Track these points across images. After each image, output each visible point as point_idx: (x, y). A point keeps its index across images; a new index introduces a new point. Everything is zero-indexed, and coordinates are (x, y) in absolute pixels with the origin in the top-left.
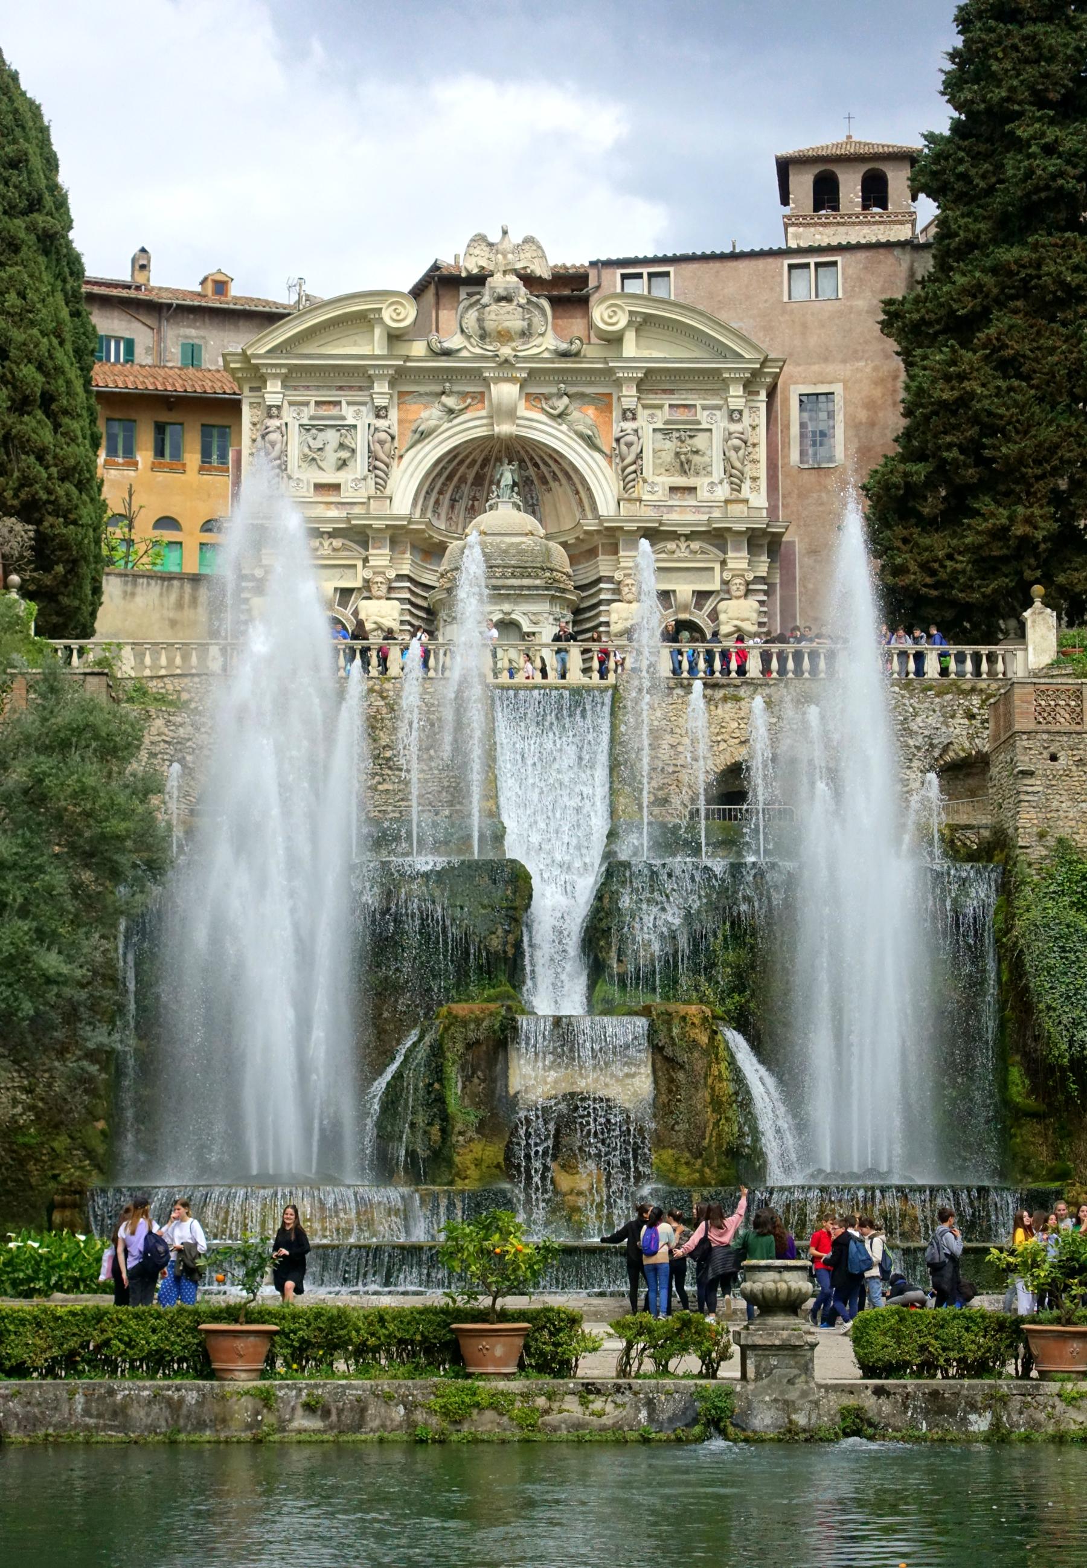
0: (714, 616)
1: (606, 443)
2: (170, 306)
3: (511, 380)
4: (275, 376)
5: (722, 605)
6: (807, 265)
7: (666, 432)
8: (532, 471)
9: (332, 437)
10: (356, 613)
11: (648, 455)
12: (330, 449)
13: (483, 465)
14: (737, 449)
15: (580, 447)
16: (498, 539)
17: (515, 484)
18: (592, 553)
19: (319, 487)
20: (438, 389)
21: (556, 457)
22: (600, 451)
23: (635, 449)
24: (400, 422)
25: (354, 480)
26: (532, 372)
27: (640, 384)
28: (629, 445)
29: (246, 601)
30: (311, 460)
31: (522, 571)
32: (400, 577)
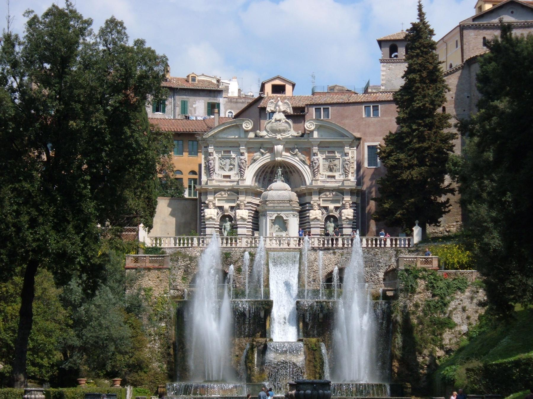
0: (340, 213)
2: (177, 89)
5: (343, 211)
8: (287, 169)
9: (228, 161)
10: (235, 213)
12: (227, 165)
13: (273, 168)
15: (301, 164)
16: (277, 192)
17: (282, 174)
18: (304, 195)
22: (307, 165)
23: (317, 164)
24: (248, 156)
28: (315, 163)
29: (203, 210)
31: (283, 201)
32: (248, 203)
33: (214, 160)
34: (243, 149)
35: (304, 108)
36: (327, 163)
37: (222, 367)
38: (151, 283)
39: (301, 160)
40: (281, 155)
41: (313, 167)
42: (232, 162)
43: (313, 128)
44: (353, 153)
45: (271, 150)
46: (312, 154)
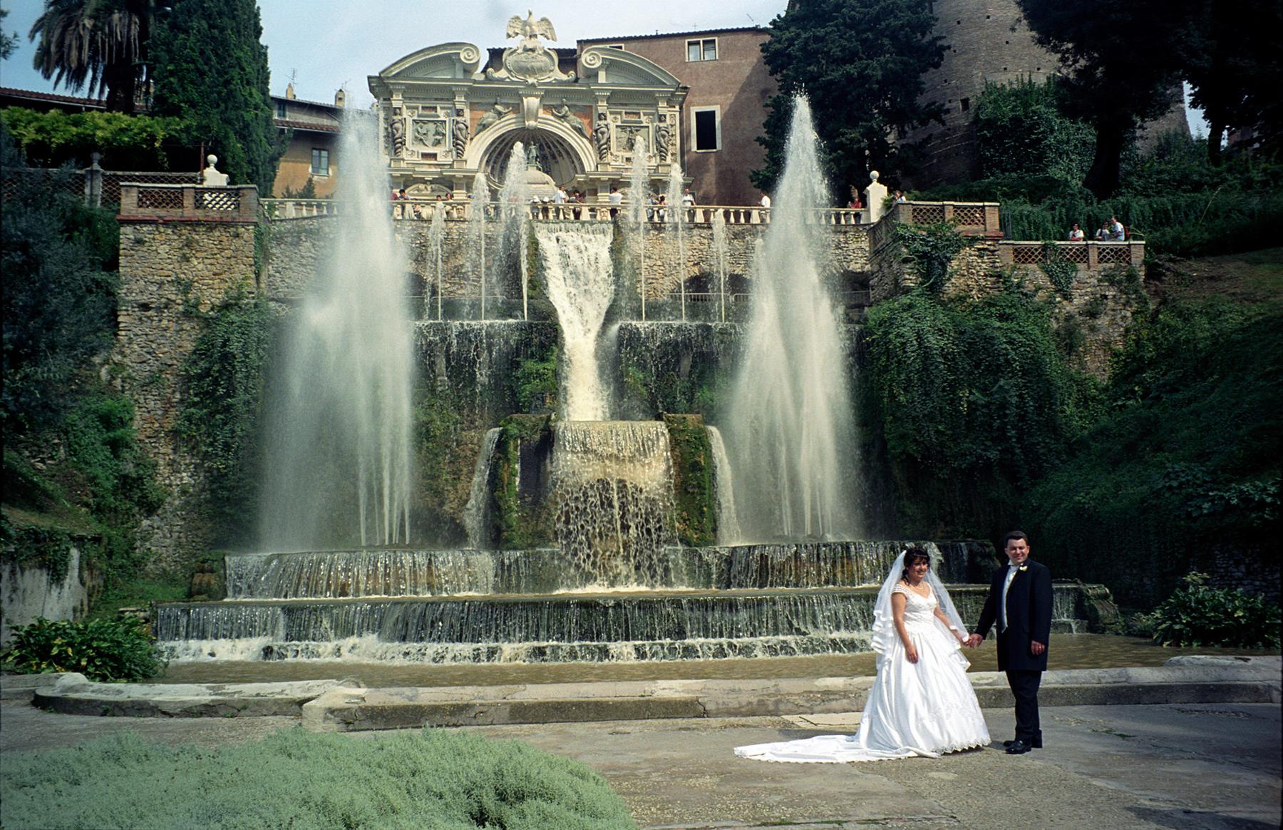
1: (588, 132)
3: (536, 96)
4: (398, 90)
6: (698, 43)
7: (623, 128)
8: (547, 151)
9: (431, 127)
11: (613, 139)
14: (664, 136)
15: (575, 135)
19: (425, 156)
20: (493, 101)
21: (561, 141)
24: (472, 119)
25: (444, 153)
26: (547, 91)
27: (608, 99)
28: (603, 133)
30: (419, 140)
33: (403, 122)
34: (460, 102)
35: (574, 51)
36: (625, 136)
37: (407, 511)
38: (200, 266)
39: (575, 128)
40: (536, 118)
41: (598, 140)
42: (440, 130)
43: (598, 64)
44: (673, 117)
45: (517, 108)
46: (595, 116)
